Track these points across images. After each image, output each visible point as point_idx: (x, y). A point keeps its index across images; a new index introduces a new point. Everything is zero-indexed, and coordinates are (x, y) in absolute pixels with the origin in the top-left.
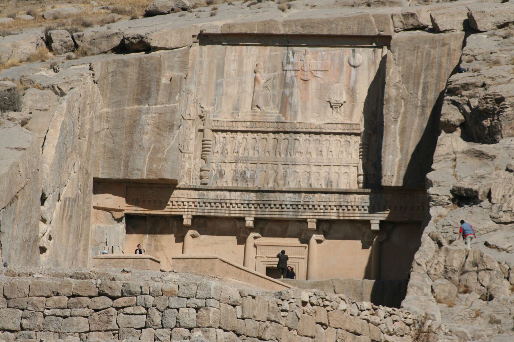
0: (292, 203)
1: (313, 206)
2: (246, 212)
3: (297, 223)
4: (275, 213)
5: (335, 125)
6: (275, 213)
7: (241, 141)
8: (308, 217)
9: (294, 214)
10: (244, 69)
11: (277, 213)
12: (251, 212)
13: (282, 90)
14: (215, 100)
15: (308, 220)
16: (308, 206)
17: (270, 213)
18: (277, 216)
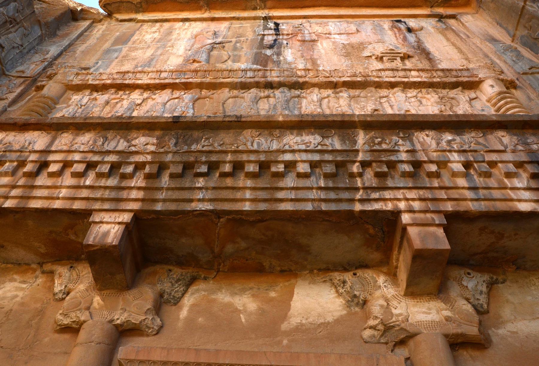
0: (316, 157)
1: (417, 165)
2: (98, 194)
3: (337, 276)
4: (239, 195)
5: (401, 74)
6: (239, 195)
7: (139, 102)
8: (402, 205)
9: (332, 195)
10: (174, 37)
11: (248, 195)
12: (124, 194)
13: (255, 51)
14: (97, 63)
15: (406, 218)
16: (392, 165)
17: (209, 195)
18: (247, 207)
